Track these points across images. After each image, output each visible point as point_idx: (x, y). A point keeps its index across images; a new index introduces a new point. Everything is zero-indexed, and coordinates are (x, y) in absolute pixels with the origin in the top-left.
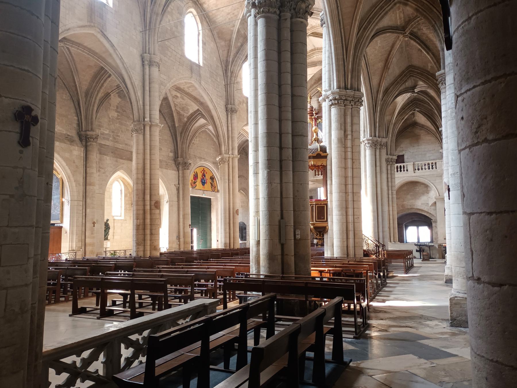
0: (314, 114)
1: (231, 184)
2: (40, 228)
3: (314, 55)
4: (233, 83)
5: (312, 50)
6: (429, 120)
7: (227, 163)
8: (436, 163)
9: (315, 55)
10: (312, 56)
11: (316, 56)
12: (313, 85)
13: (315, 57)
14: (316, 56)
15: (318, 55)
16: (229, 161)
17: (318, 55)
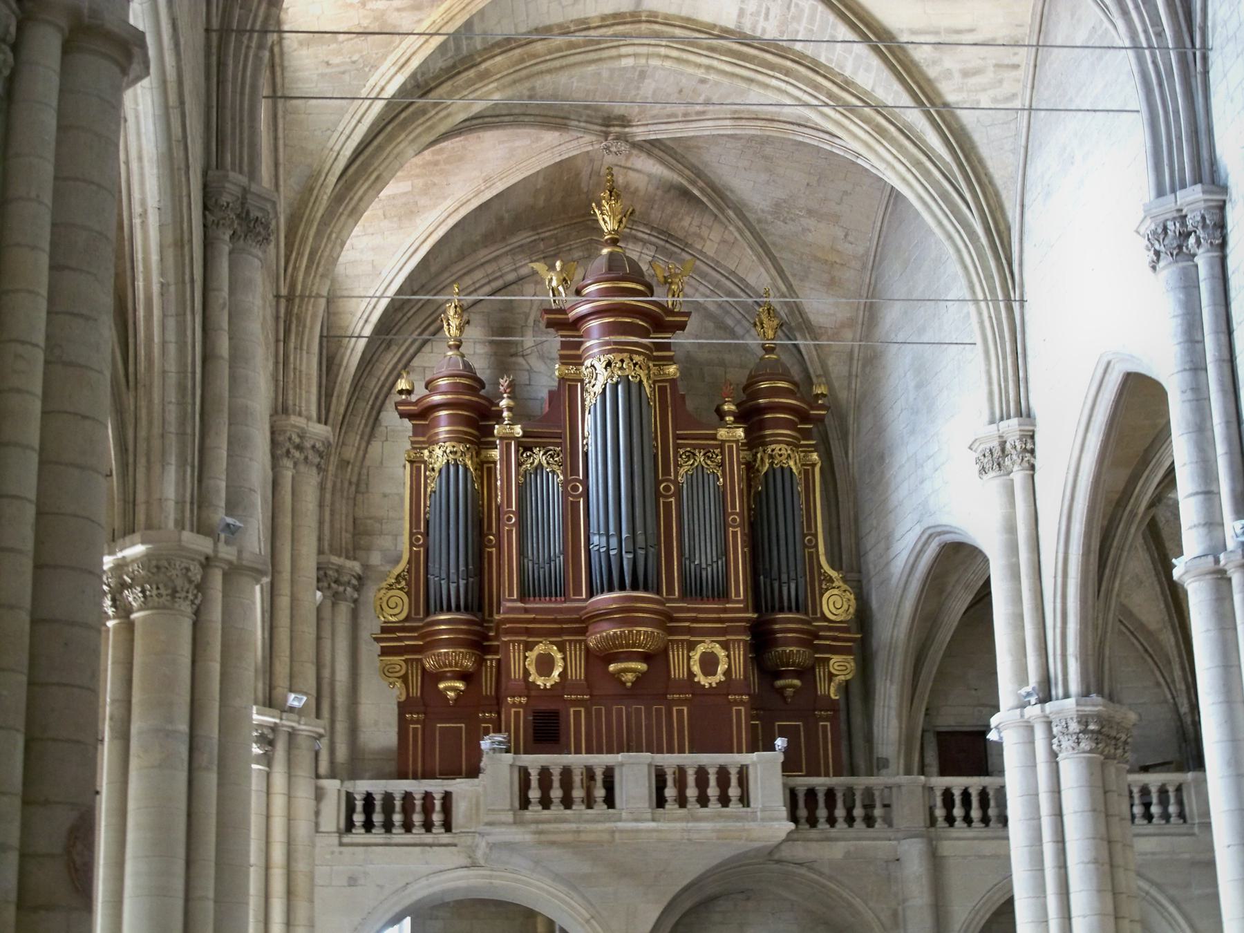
0: (505, 414)
1: (210, 780)
2: (1114, 791)
3: (623, 50)
4: (258, 27)
5: (615, 16)
6: (1148, 549)
7: (187, 608)
8: (1179, 789)
9: (630, 50)
10: (614, 52)
11: (635, 55)
12: (474, 247)
13: (628, 62)
14: (635, 55)
15: (648, 56)
16: (201, 587)
17: (648, 56)
